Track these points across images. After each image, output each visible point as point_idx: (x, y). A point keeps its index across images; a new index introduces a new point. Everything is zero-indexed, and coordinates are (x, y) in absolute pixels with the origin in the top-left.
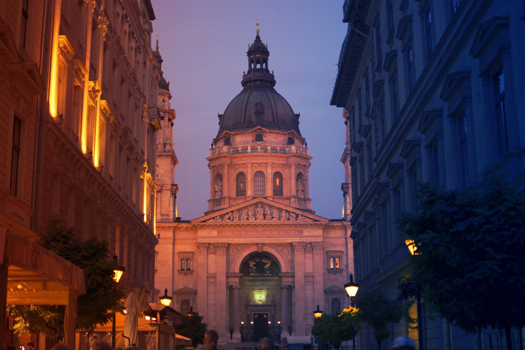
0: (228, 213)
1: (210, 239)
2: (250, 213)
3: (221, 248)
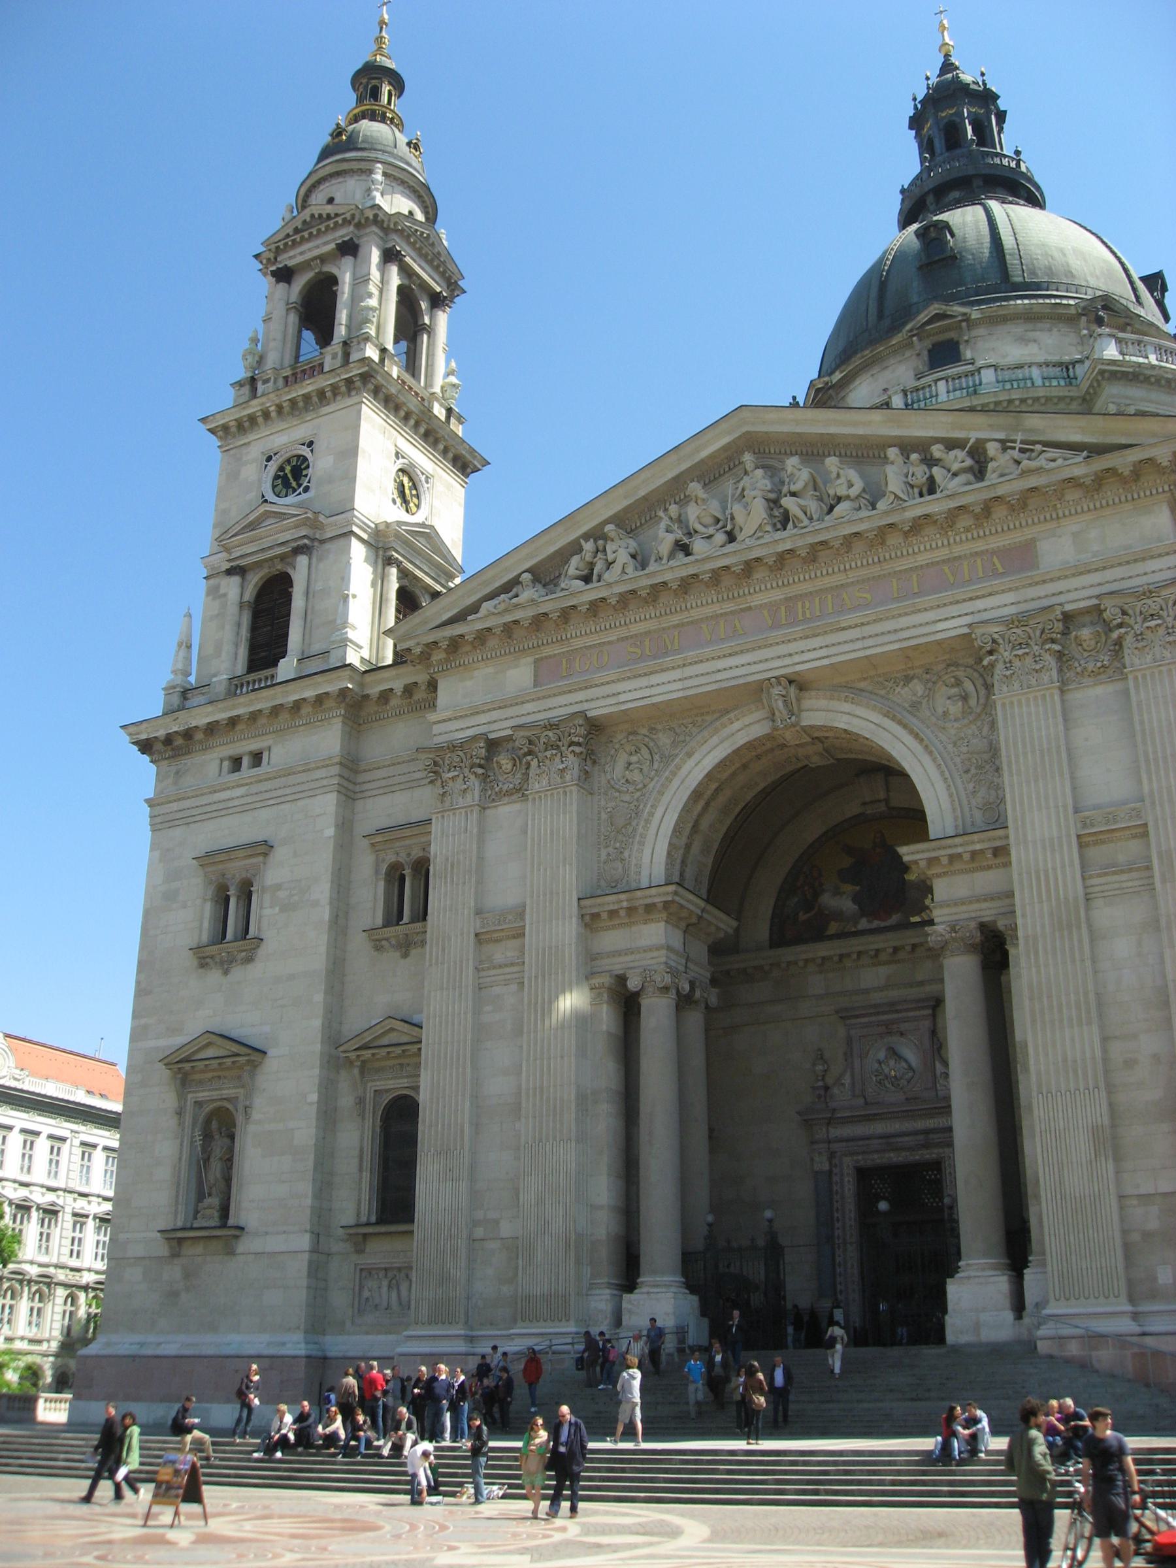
0: (575, 548)
1: (495, 715)
2: (693, 513)
3: (548, 754)
